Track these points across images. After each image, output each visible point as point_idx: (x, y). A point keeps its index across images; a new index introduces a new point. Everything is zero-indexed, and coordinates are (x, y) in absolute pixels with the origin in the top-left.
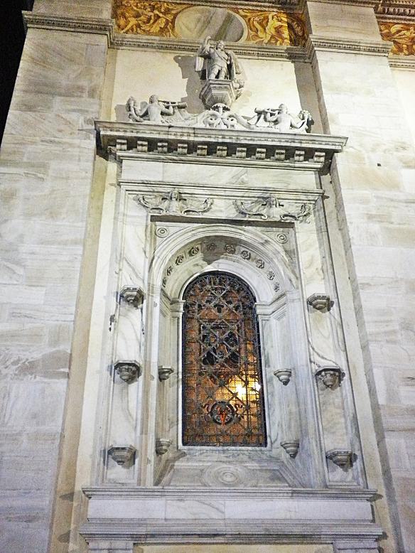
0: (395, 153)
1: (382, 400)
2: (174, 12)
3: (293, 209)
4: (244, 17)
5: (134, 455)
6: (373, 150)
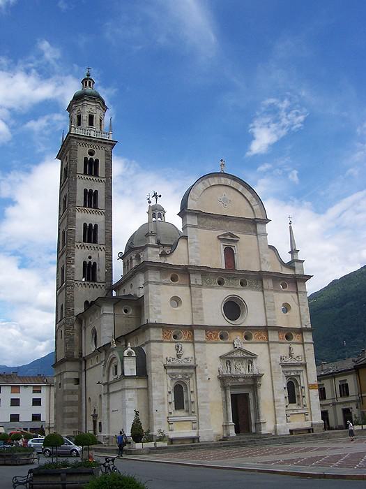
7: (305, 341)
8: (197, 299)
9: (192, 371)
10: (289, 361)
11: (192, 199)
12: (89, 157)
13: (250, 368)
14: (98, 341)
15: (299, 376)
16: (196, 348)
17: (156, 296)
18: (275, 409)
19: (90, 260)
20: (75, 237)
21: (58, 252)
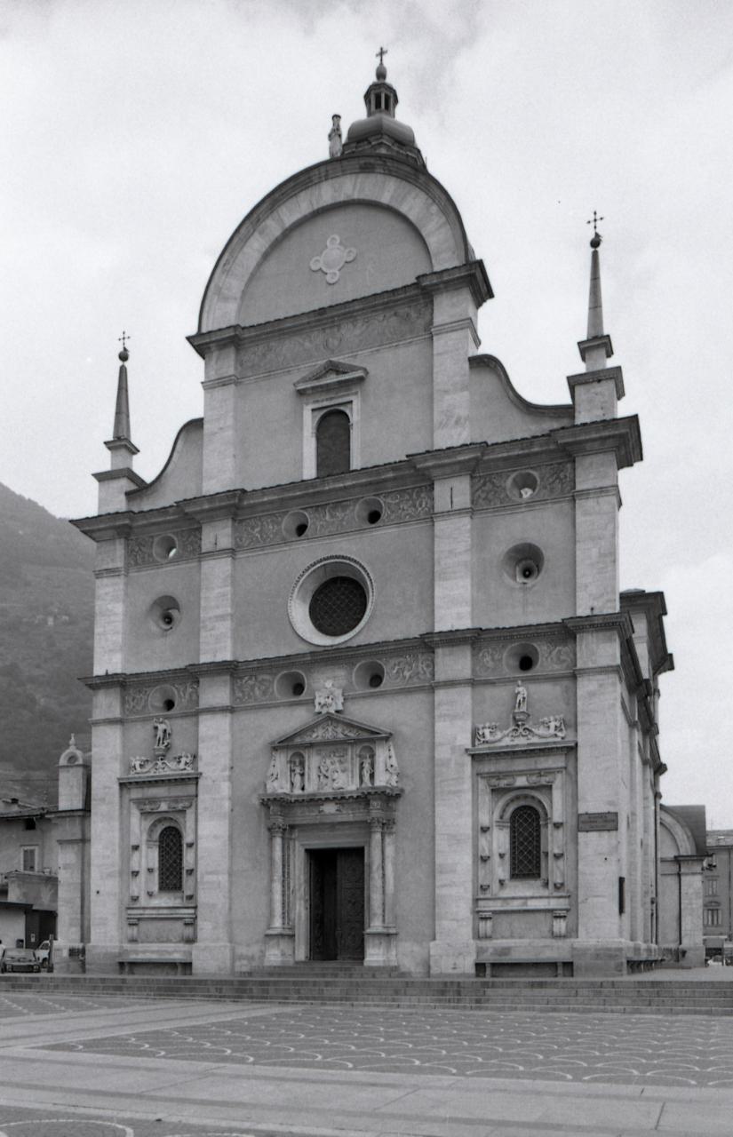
3: (187, 804)
5: (138, 897)
9: (190, 789)
15: (549, 787)
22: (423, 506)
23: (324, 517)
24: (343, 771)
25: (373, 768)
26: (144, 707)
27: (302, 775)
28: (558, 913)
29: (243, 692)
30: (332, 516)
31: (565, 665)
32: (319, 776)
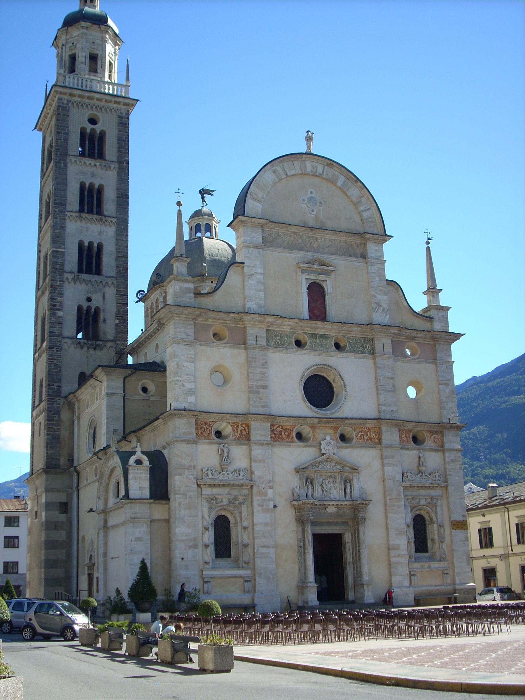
0: (268, 484)
1: (256, 551)
2: (211, 425)
3: (241, 501)
4: (232, 426)
6: (263, 483)
7: (447, 445)
8: (259, 370)
10: (417, 480)
11: (254, 199)
12: (89, 127)
13: (348, 490)
14: (97, 440)
16: (253, 453)
17: (185, 364)
18: (389, 561)
19: (89, 304)
20: (63, 264)
21: (38, 288)
22: (367, 348)
23: (317, 341)
24: (335, 489)
25: (351, 488)
26: (209, 434)
27: (313, 489)
28: (445, 572)
29: (275, 434)
30: (320, 342)
31: (437, 444)
32: (323, 491)
